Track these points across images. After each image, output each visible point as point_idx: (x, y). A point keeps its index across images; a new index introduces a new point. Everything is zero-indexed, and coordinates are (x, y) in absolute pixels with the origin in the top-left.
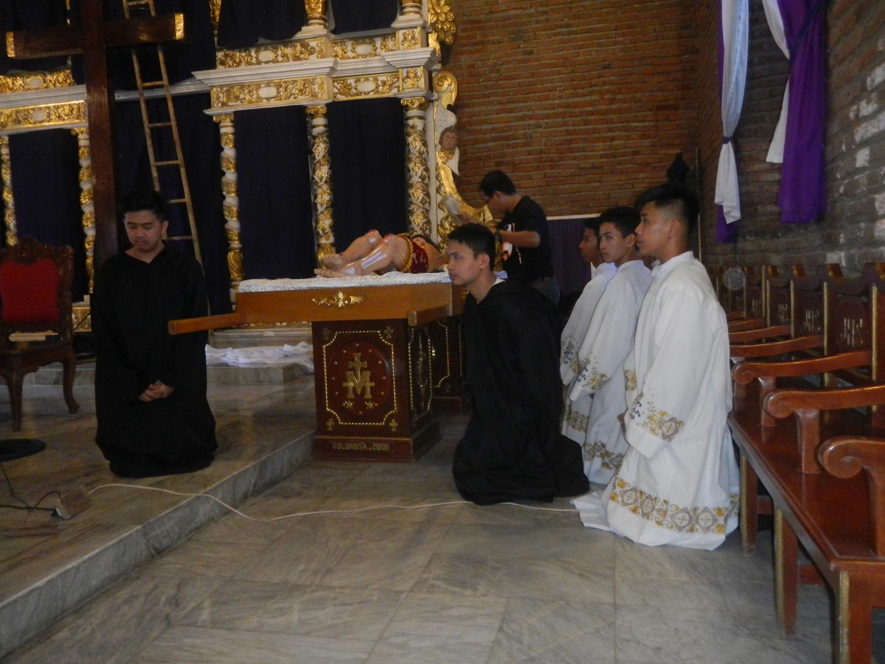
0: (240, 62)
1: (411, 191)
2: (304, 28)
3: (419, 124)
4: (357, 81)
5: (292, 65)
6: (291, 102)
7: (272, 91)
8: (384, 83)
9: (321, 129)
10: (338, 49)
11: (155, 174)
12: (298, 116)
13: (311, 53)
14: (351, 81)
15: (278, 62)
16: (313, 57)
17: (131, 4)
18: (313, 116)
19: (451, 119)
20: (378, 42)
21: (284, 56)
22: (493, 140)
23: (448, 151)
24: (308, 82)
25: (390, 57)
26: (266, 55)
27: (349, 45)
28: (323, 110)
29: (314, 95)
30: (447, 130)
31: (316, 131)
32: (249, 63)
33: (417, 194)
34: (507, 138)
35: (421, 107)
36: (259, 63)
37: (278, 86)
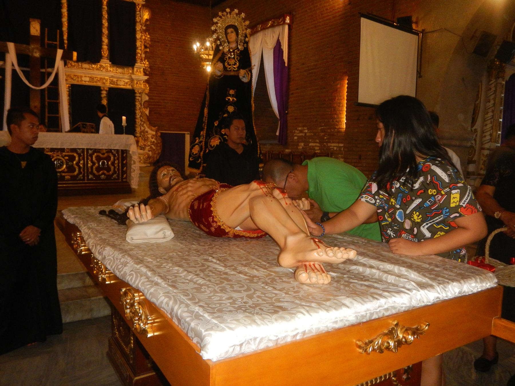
0: (74, 66)
1: (137, 120)
2: (102, 60)
3: (139, 98)
4: (117, 81)
5: (96, 72)
6: (94, 84)
7: (88, 79)
8: (127, 83)
9: (105, 95)
10: (112, 69)
11: (47, 104)
12: (98, 89)
13: (103, 69)
14: (115, 80)
15: (90, 69)
16: (104, 70)
17: (49, 42)
18: (102, 90)
19: (147, 98)
20: (126, 70)
21: (93, 68)
22: (154, 105)
23: (146, 107)
24: (101, 78)
25: (133, 77)
26: (85, 66)
27: (115, 69)
28: (107, 89)
29: (104, 83)
30: (146, 101)
31: (103, 96)
32: (79, 68)
33: (138, 121)
34: (159, 105)
35: (140, 93)
36: (82, 68)
37: (91, 77)
